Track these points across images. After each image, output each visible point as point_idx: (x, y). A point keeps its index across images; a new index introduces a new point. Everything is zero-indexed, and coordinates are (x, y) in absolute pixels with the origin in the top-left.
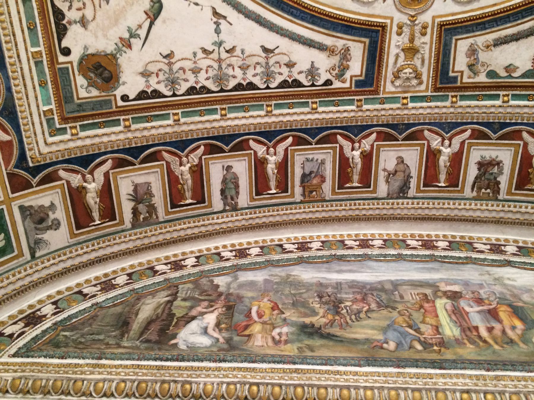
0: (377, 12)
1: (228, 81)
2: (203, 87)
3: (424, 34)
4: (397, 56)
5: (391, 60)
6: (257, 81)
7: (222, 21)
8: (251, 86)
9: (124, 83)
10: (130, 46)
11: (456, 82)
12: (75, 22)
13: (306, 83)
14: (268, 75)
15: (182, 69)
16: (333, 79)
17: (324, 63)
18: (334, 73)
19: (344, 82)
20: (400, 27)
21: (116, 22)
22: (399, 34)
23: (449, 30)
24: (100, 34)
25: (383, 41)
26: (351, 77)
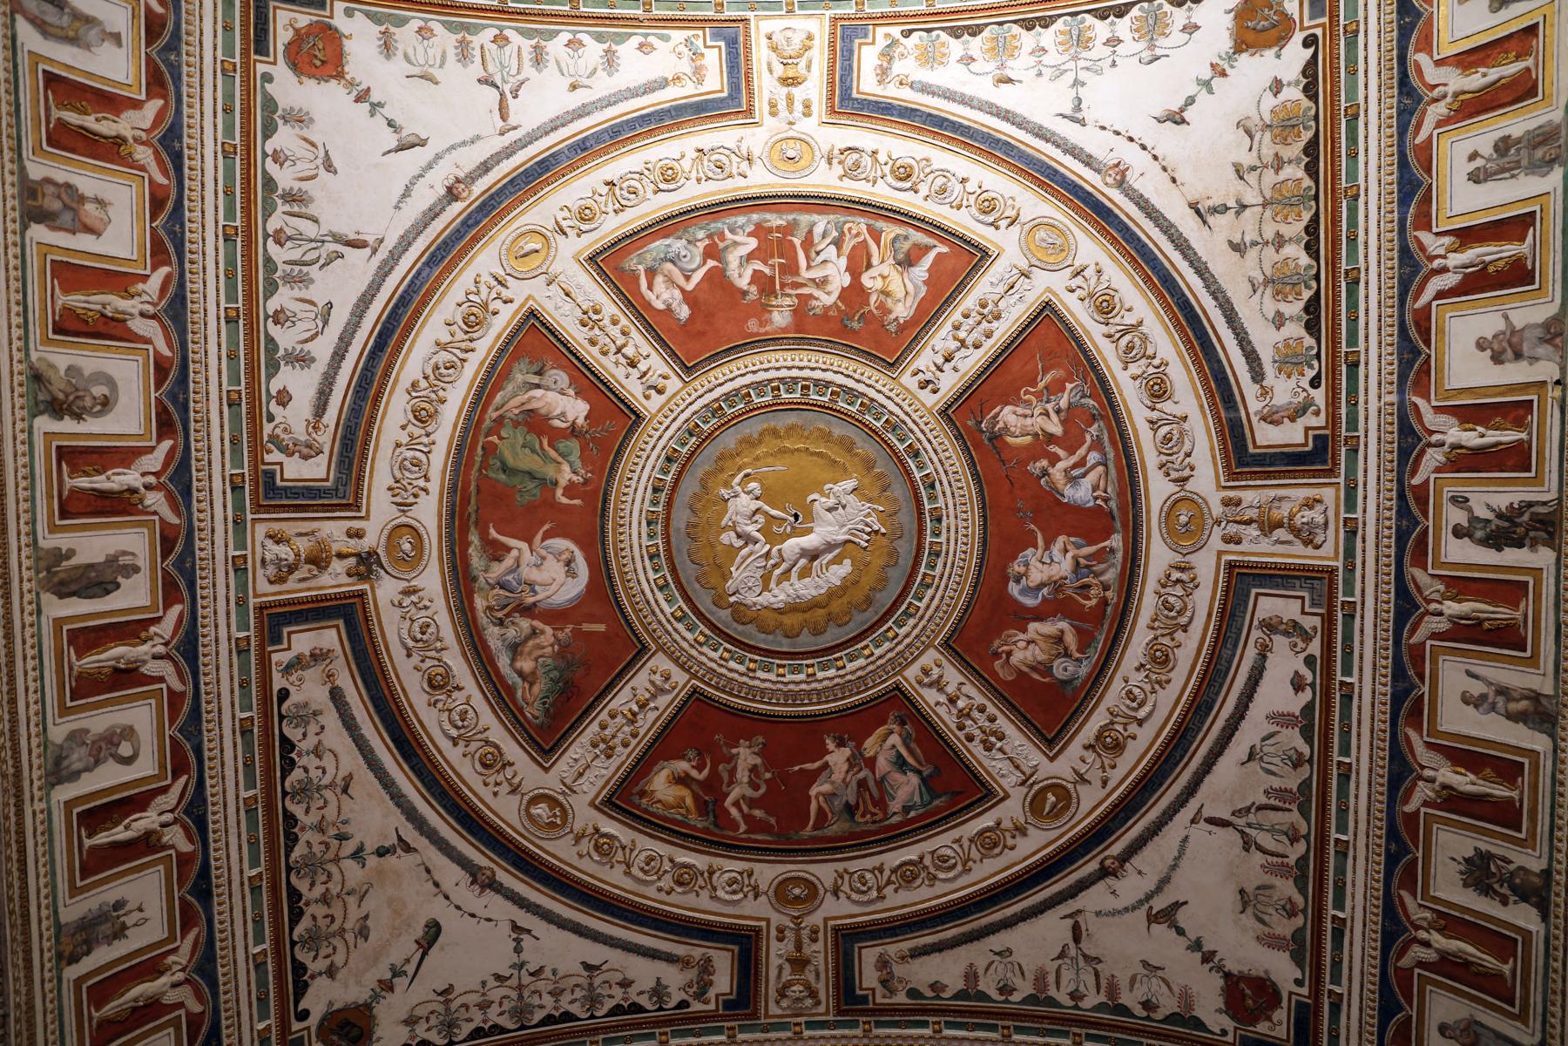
0: (746, 912)
1: (532, 1013)
2: (495, 1026)
3: (815, 940)
4: (780, 968)
5: (773, 973)
6: (575, 1009)
7: (524, 936)
8: (568, 1016)
9: (379, 1039)
10: (391, 989)
11: (867, 1003)
12: (320, 974)
13: (650, 1007)
14: (593, 1000)
15: (466, 1006)
16: (690, 1000)
17: (675, 980)
18: (691, 991)
19: (706, 1002)
20: (781, 930)
21: (376, 960)
22: (780, 940)
23: (848, 938)
24: (352, 981)
25: (758, 949)
26: (717, 996)
